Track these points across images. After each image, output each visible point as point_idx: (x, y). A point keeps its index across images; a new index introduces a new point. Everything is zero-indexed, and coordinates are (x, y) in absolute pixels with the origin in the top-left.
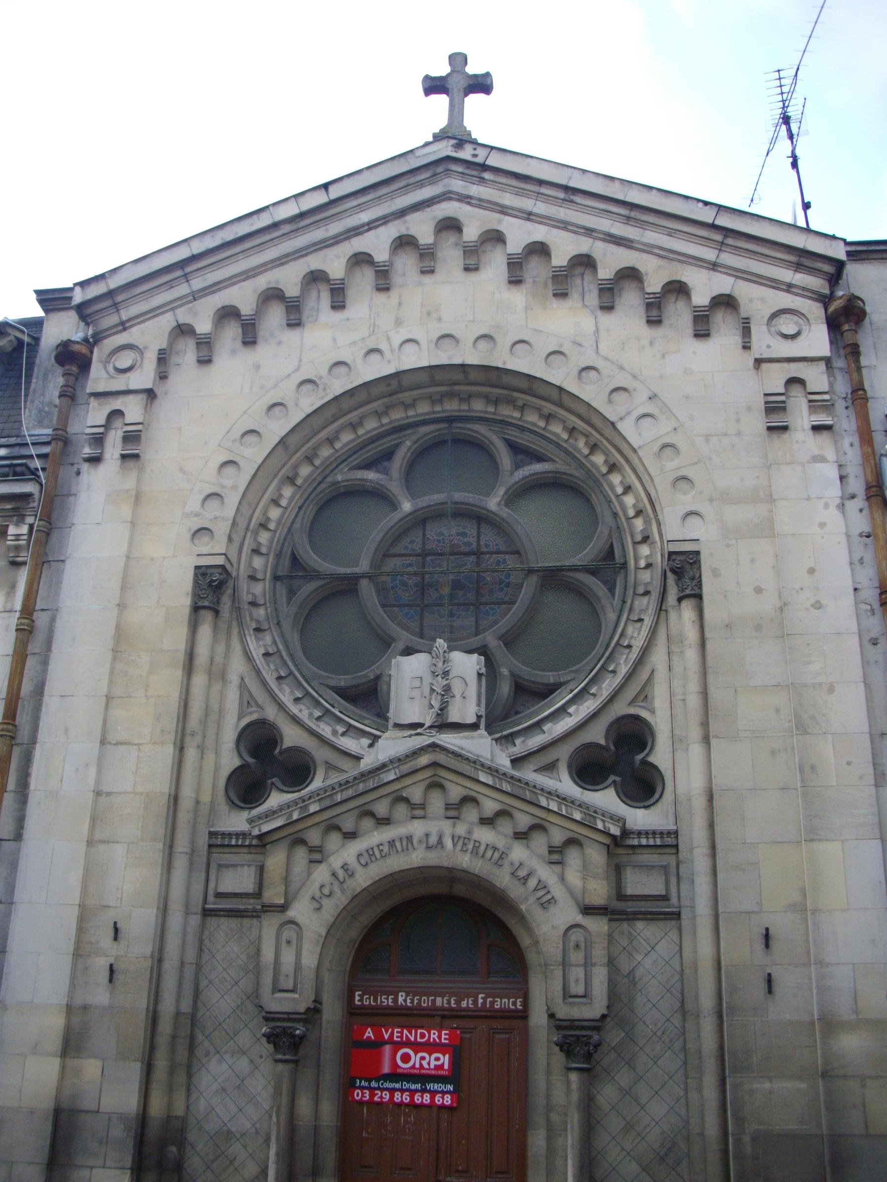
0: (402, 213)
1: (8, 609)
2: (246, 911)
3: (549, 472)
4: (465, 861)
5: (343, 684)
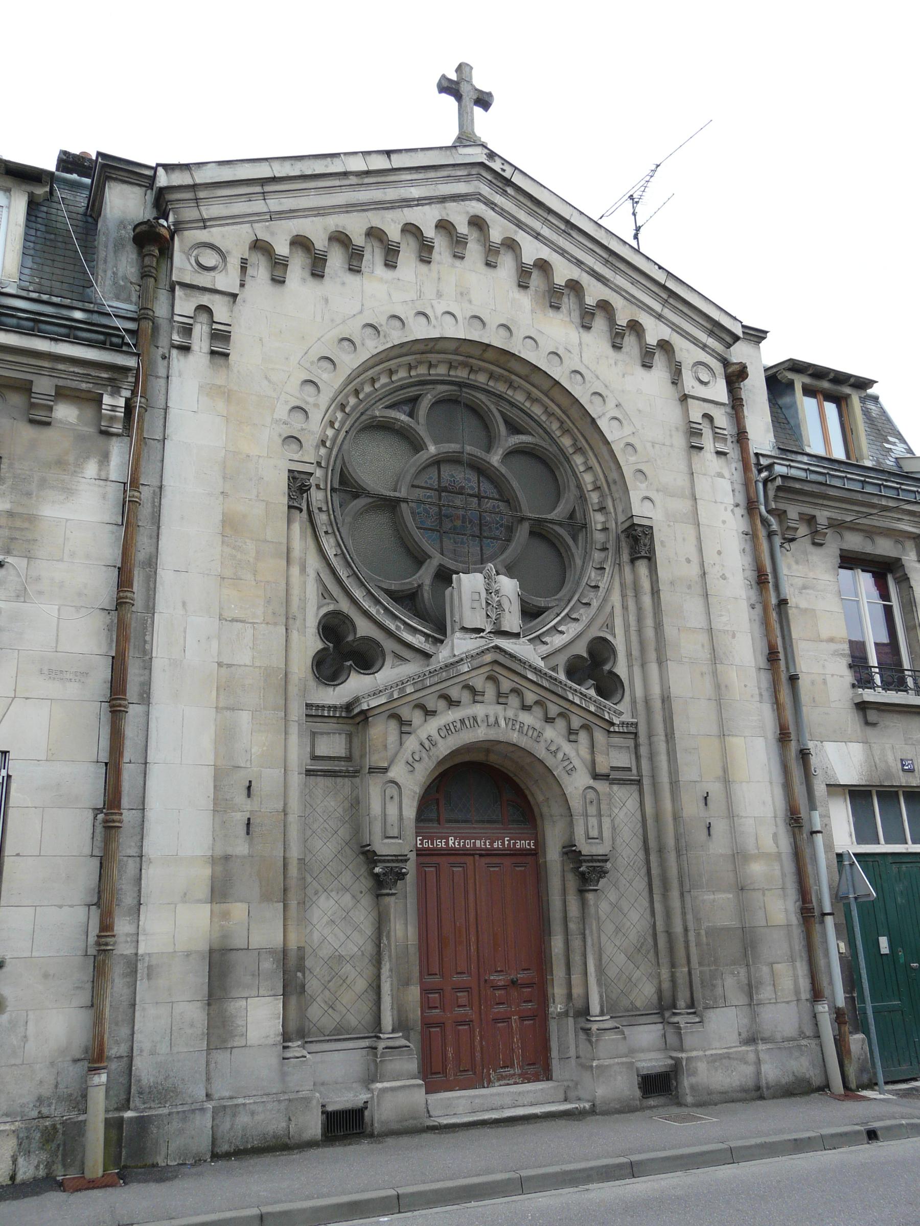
0: (443, 199)
1: (103, 477)
2: (340, 771)
3: (532, 444)
4: (514, 737)
5: (393, 588)
